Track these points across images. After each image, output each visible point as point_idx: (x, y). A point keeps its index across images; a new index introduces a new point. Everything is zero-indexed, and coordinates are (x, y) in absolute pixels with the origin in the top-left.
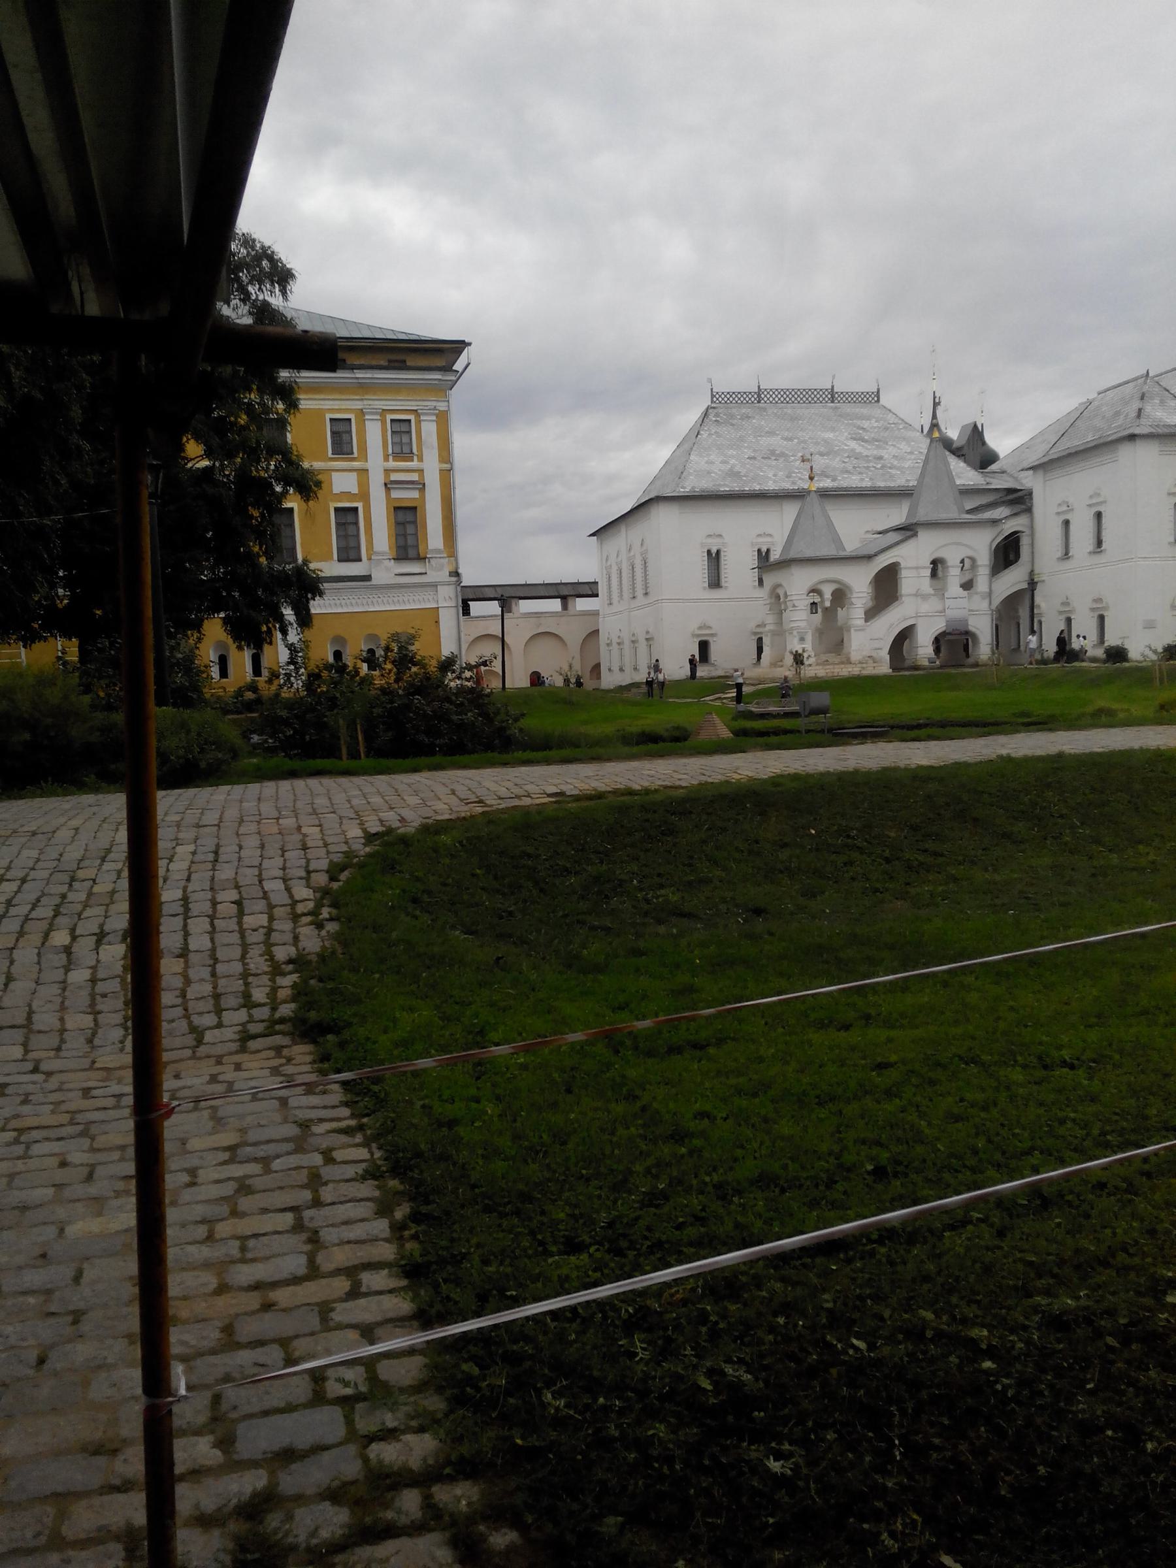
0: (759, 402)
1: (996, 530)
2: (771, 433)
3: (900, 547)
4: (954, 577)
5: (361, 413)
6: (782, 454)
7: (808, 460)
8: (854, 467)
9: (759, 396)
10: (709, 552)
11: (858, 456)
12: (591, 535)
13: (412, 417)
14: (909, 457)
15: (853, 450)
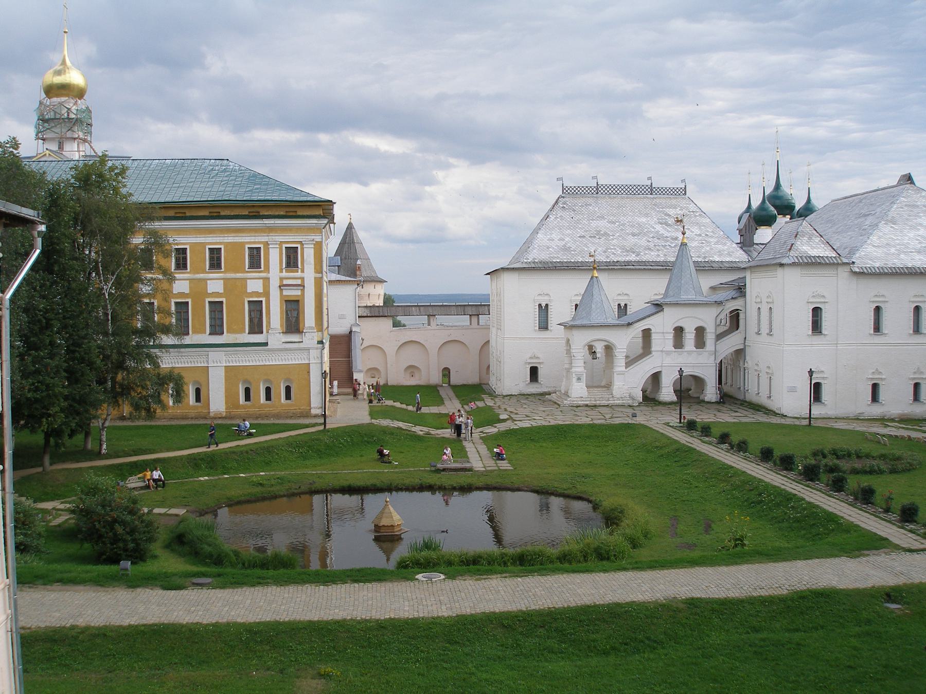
0: (597, 193)
1: (720, 309)
2: (603, 218)
3: (650, 319)
4: (690, 338)
5: (267, 244)
6: (606, 234)
7: (592, 256)
8: (655, 245)
9: (597, 189)
10: (540, 305)
11: (660, 237)
12: (486, 274)
13: (298, 246)
14: (697, 238)
15: (658, 232)
